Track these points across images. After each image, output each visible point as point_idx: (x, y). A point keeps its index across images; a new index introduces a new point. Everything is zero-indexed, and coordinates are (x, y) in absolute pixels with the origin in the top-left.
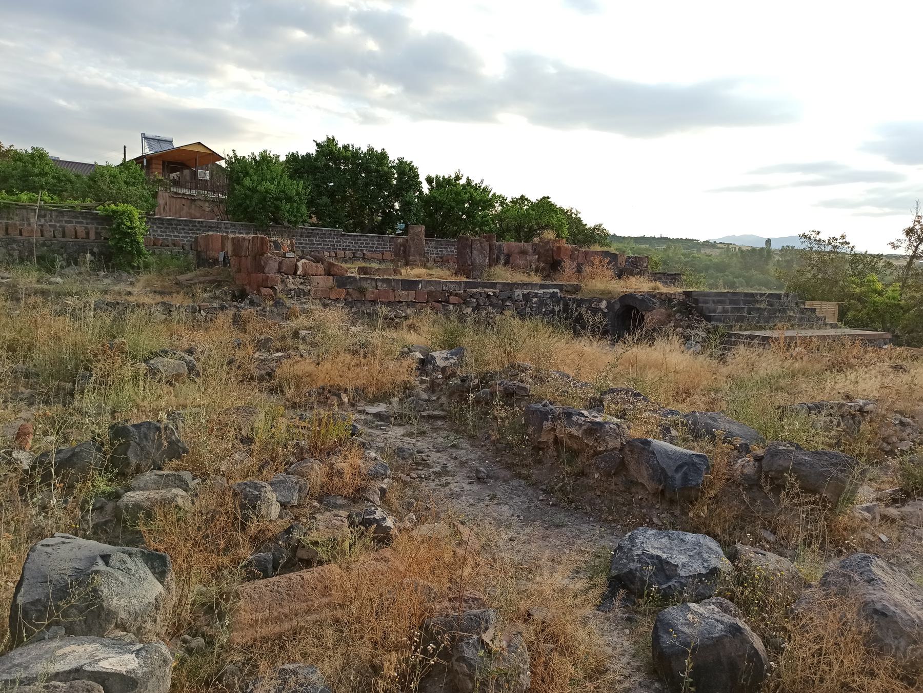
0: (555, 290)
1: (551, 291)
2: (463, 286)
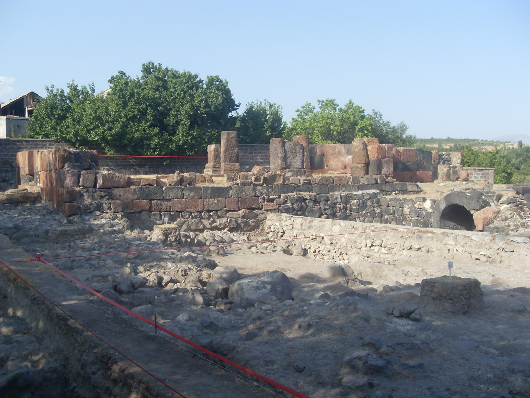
1: (371, 191)
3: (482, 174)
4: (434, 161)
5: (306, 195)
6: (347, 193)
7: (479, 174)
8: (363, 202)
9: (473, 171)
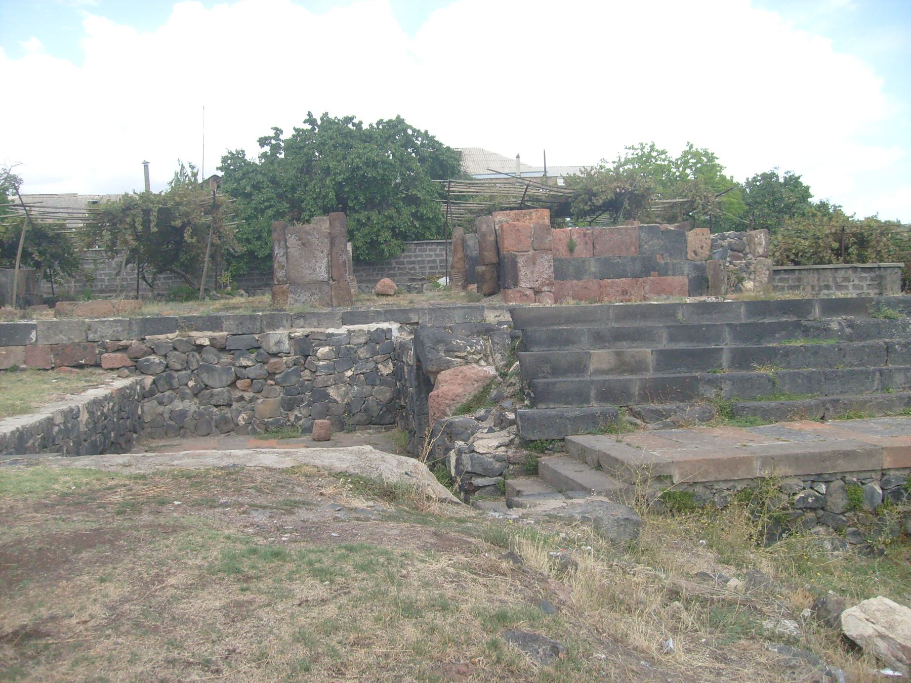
0: (385, 326)
1: (373, 327)
2: (135, 328)
3: (872, 280)
4: (695, 253)
5: (203, 338)
6: (308, 330)
7: (865, 278)
8: (348, 350)
9: (850, 272)
